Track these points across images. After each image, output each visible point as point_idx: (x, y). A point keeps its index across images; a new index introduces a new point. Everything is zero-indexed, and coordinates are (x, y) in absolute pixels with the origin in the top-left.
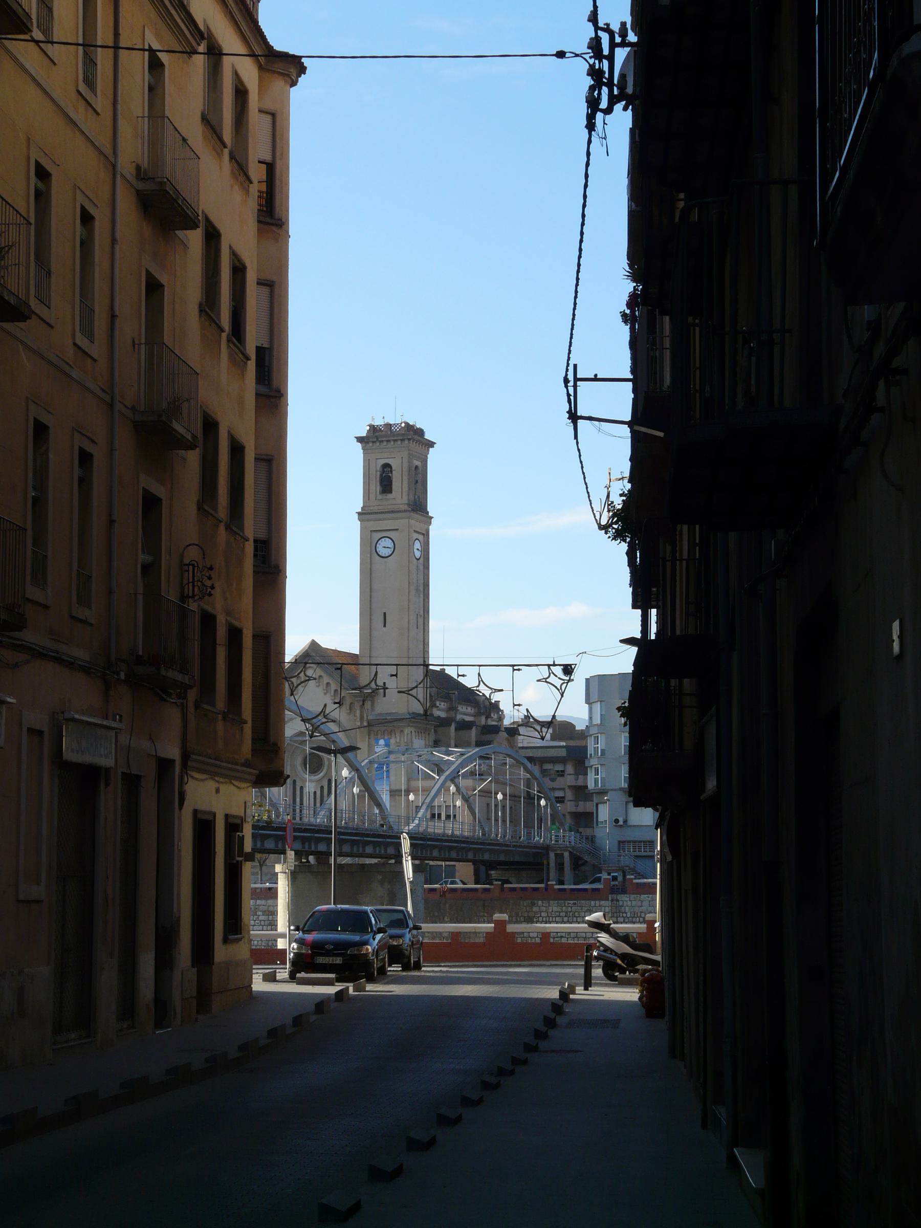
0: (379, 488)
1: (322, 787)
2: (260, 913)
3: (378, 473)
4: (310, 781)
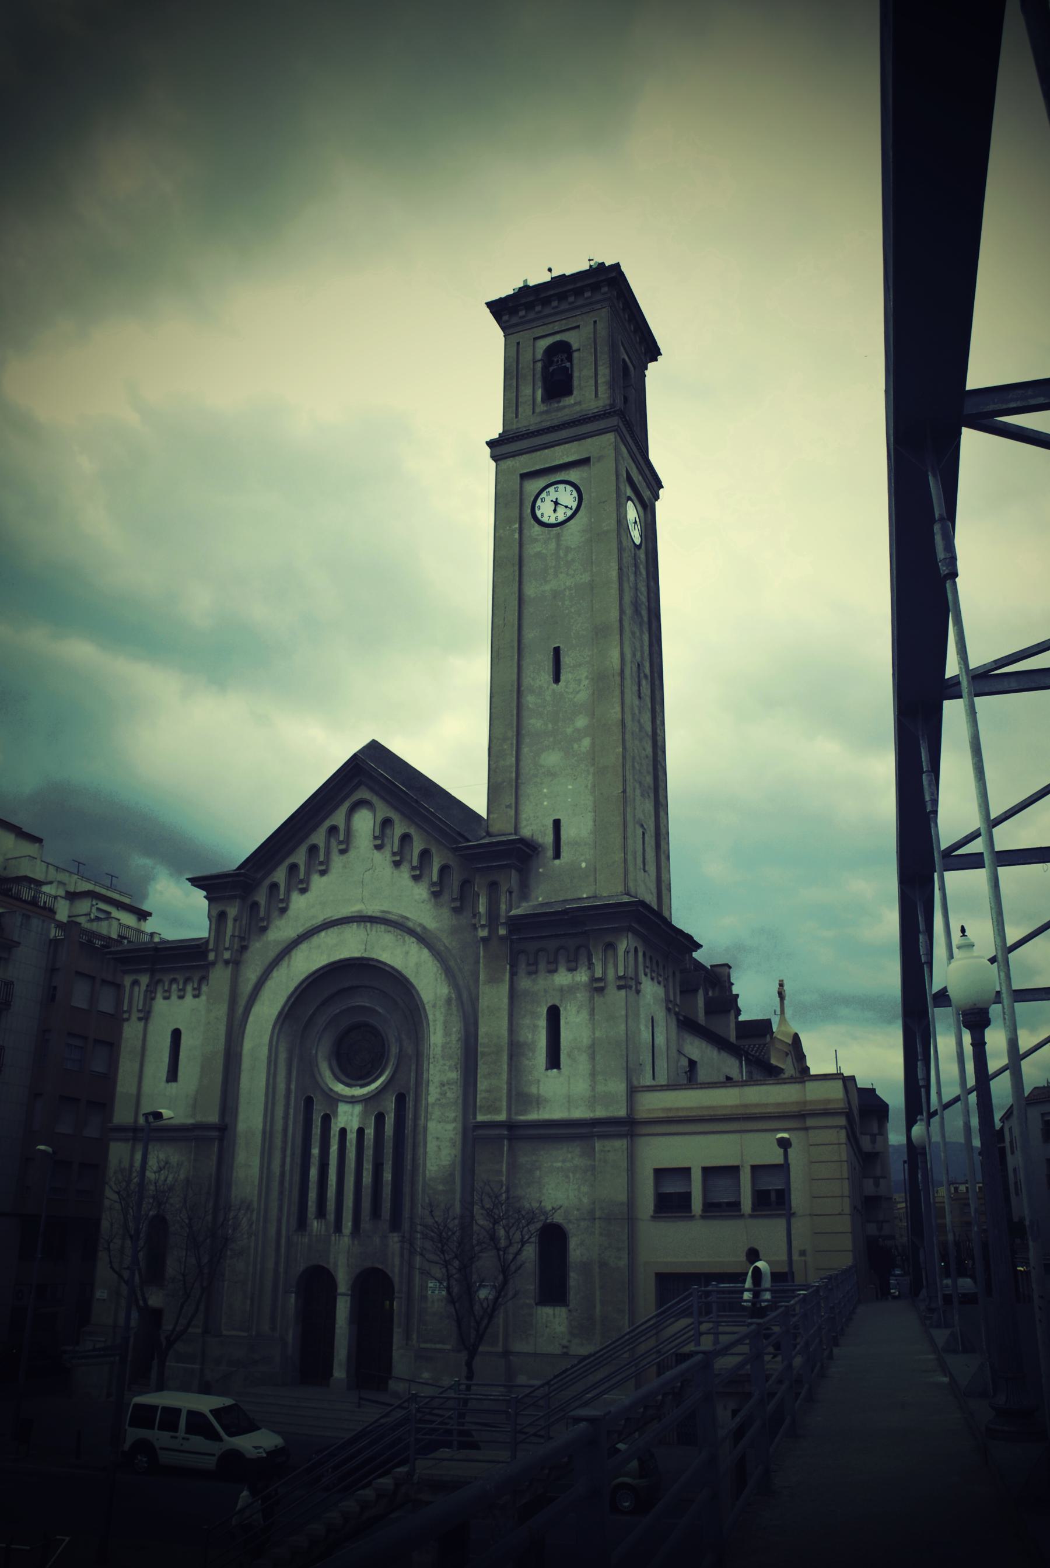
0: (539, 393)
1: (380, 1118)
3: (539, 365)
4: (352, 1101)
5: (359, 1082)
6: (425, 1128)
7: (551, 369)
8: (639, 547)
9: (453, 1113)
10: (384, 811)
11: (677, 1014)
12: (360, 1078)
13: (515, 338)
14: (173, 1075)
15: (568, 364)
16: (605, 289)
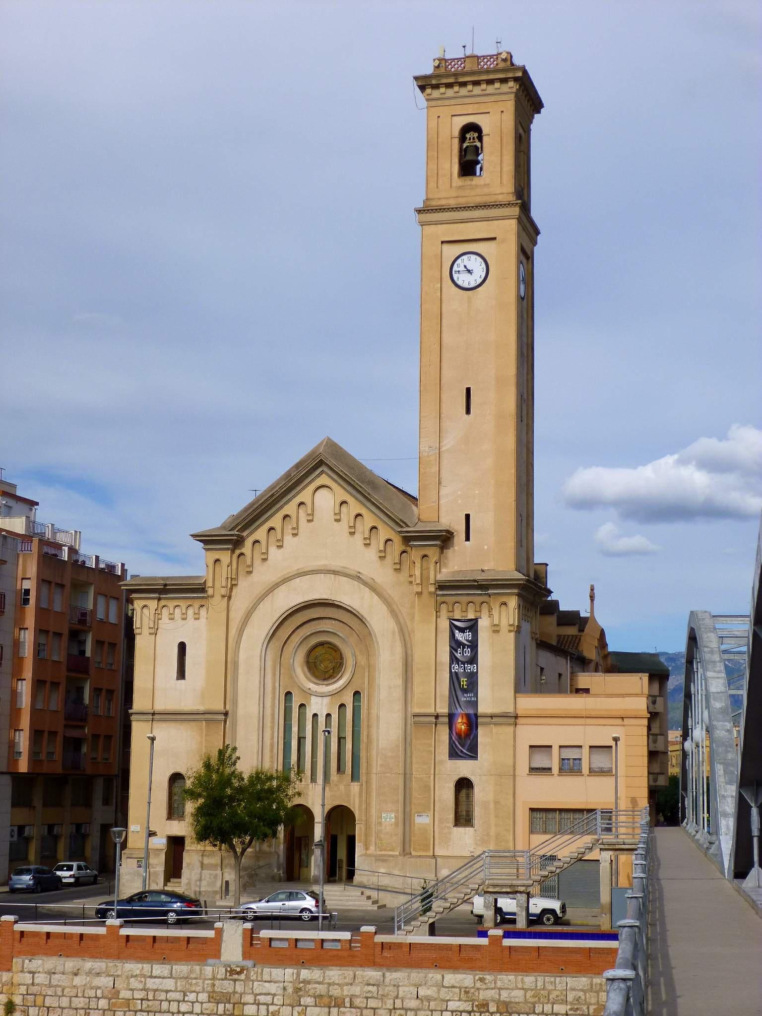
0: (456, 168)
2: (309, 1001)
3: (456, 142)
4: (322, 696)
5: (326, 683)
6: (378, 717)
7: (465, 145)
8: (523, 299)
9: (398, 706)
10: (342, 494)
11: (536, 640)
12: (325, 679)
13: (436, 111)
14: (181, 674)
15: (479, 144)
16: (511, 84)
